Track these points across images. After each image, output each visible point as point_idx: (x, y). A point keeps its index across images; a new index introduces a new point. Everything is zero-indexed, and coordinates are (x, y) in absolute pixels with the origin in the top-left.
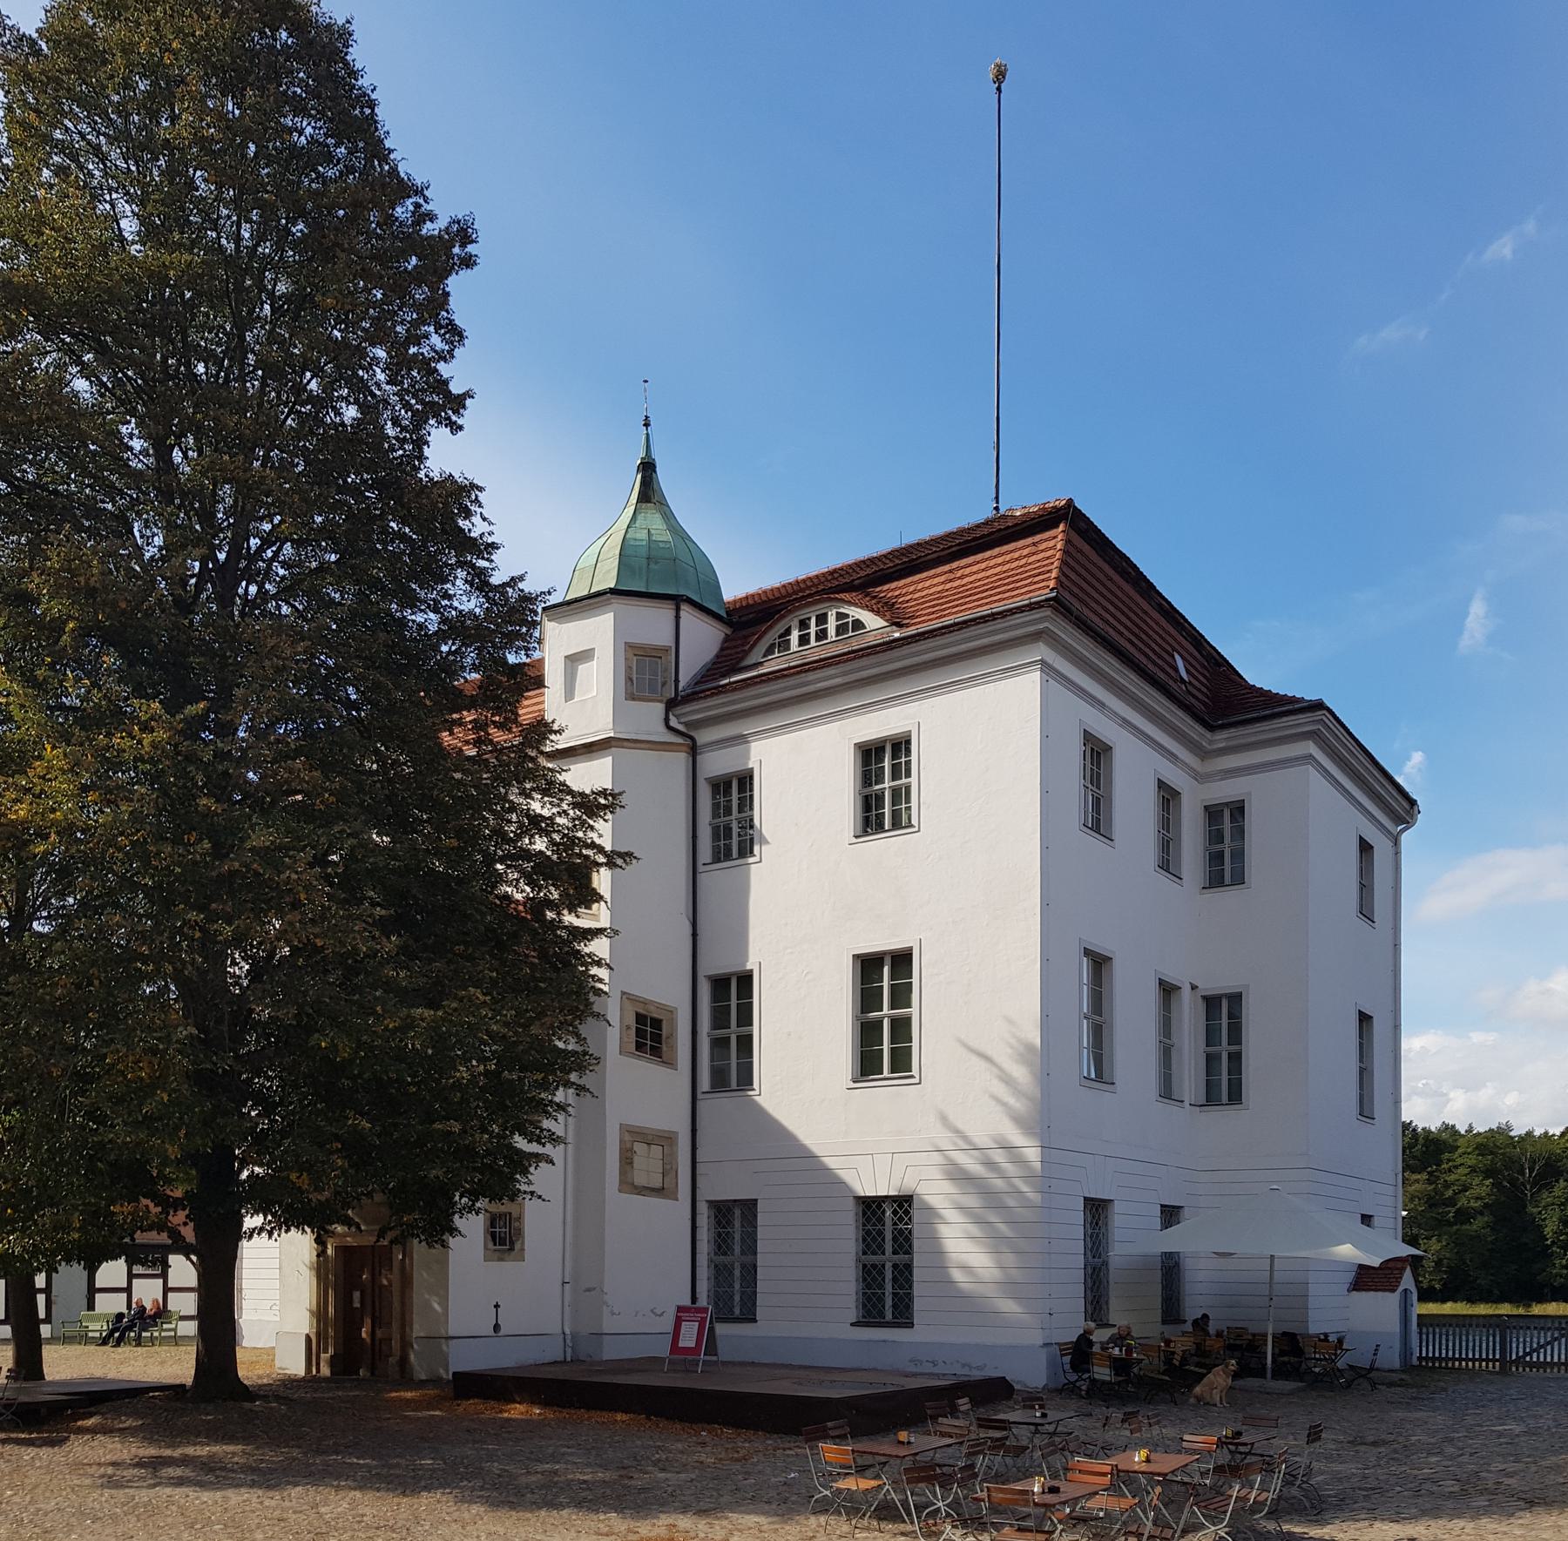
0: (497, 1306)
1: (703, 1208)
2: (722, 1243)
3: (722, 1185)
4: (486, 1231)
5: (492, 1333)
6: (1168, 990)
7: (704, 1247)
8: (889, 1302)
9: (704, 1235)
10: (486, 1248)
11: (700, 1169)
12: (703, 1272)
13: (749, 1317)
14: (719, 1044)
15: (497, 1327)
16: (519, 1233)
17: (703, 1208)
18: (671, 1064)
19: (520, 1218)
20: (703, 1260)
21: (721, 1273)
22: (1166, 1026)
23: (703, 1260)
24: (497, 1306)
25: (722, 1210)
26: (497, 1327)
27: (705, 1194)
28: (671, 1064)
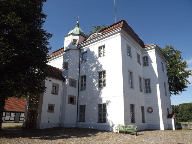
0: (49, 119)
1: (79, 106)
2: (81, 111)
3: (81, 103)
4: (48, 108)
5: (48, 122)
6: (140, 79)
7: (79, 111)
8: (103, 119)
9: (79, 110)
10: (48, 110)
11: (79, 101)
12: (78, 115)
13: (84, 121)
14: (82, 85)
15: (49, 122)
16: (54, 109)
17: (79, 106)
18: (76, 88)
19: (54, 107)
20: (78, 113)
21: (81, 115)
22: (140, 83)
23: (78, 113)
24: (49, 119)
25: (81, 106)
26: (49, 122)
27: (79, 104)
28: (75, 87)
